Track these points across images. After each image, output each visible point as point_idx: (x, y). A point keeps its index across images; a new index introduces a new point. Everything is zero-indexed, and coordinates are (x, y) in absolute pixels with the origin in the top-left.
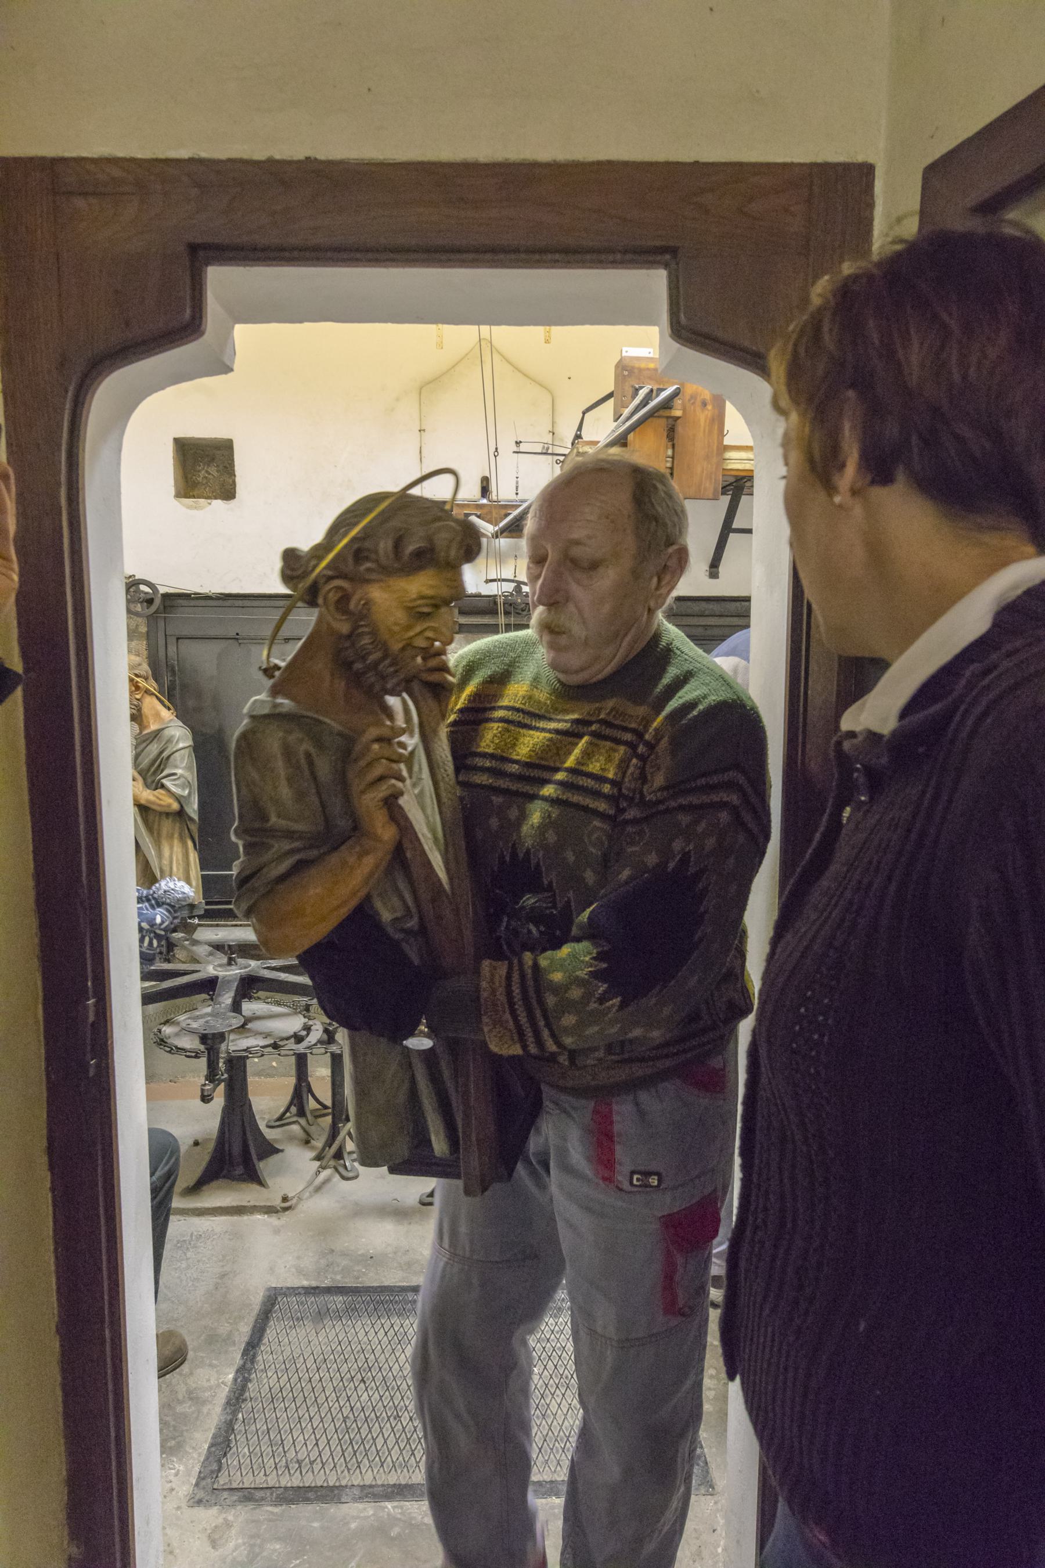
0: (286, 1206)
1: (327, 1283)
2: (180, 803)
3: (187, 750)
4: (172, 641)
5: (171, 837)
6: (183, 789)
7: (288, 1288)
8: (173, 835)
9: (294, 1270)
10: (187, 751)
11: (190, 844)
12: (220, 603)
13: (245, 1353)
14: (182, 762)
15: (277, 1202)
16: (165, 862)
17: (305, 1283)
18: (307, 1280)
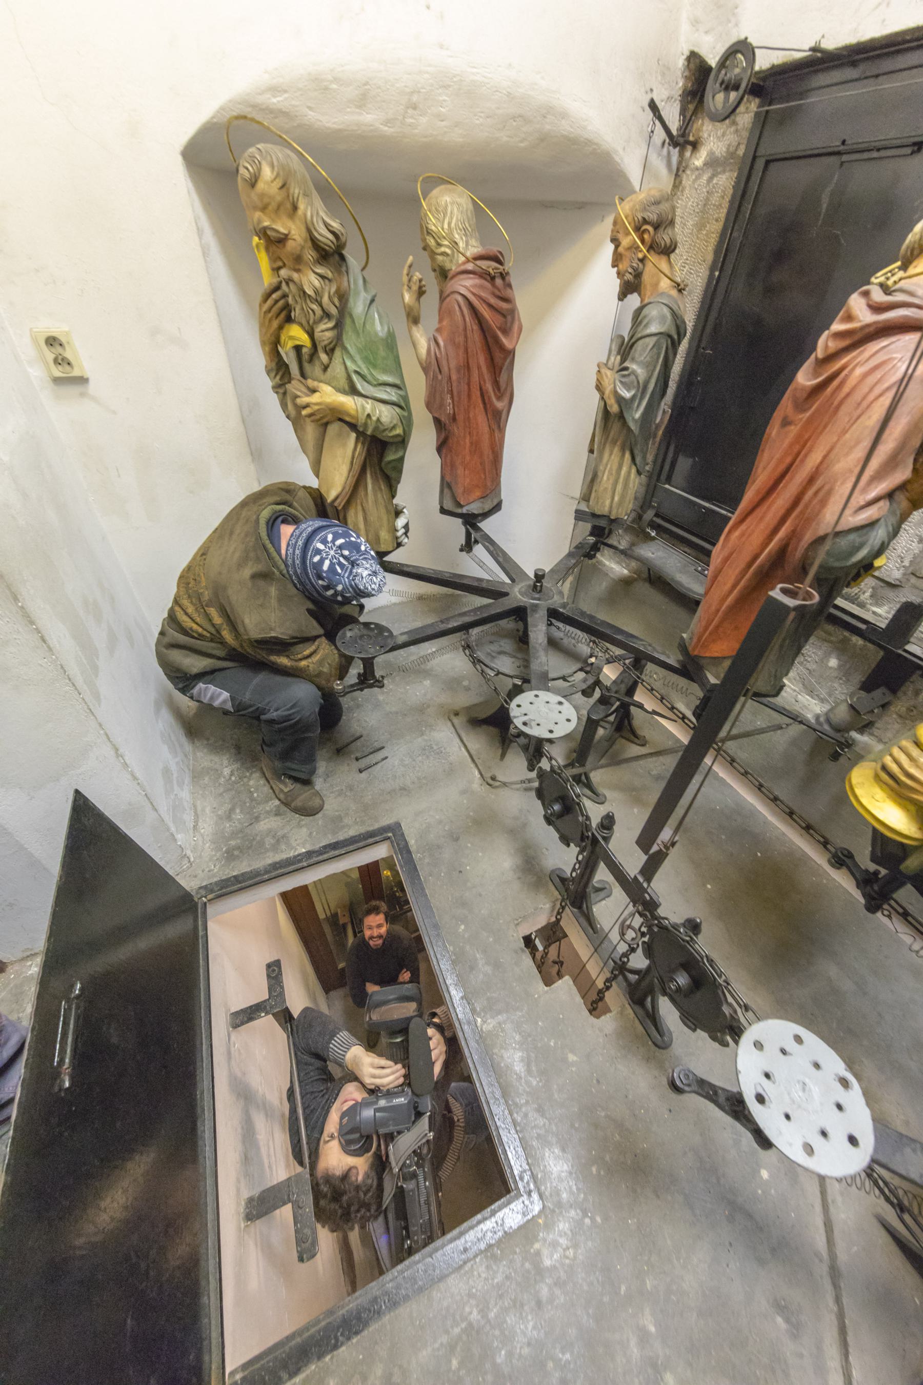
0: (491, 782)
1: (416, 856)
2: (620, 406)
3: (654, 339)
4: (760, 164)
5: (614, 443)
6: (628, 391)
7: (403, 834)
8: (617, 441)
9: (424, 826)
10: (651, 341)
11: (628, 456)
12: (850, 73)
13: (325, 847)
14: (641, 355)
15: (488, 775)
16: (601, 468)
17: (412, 842)
18: (416, 841)
